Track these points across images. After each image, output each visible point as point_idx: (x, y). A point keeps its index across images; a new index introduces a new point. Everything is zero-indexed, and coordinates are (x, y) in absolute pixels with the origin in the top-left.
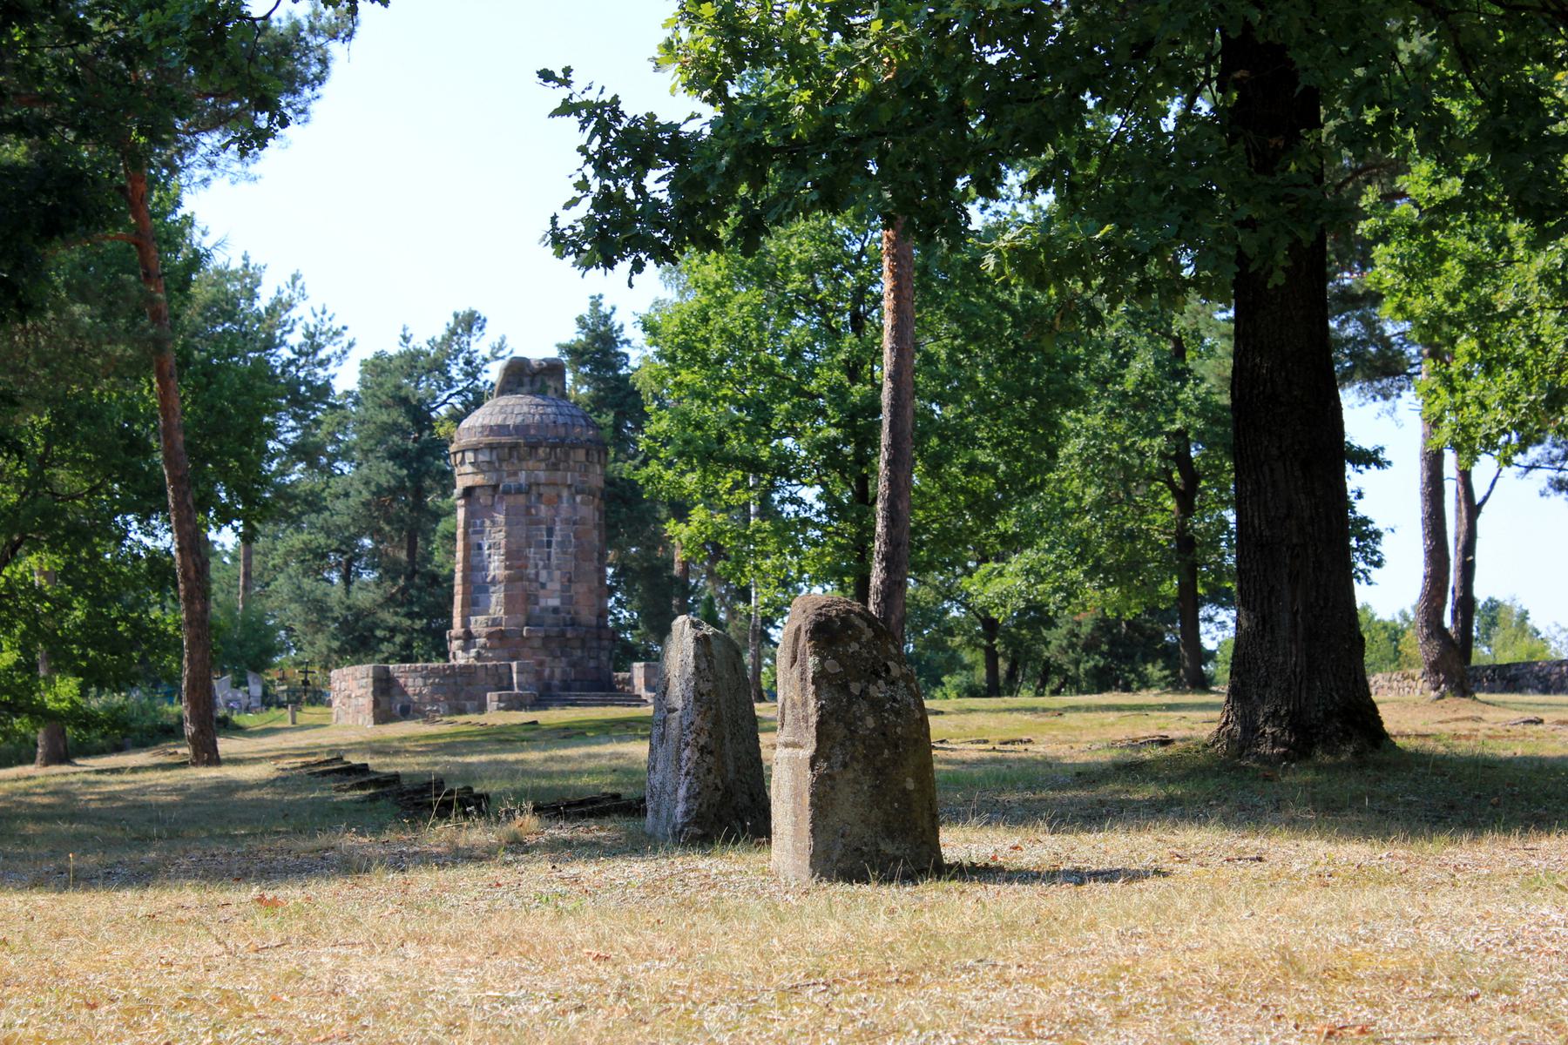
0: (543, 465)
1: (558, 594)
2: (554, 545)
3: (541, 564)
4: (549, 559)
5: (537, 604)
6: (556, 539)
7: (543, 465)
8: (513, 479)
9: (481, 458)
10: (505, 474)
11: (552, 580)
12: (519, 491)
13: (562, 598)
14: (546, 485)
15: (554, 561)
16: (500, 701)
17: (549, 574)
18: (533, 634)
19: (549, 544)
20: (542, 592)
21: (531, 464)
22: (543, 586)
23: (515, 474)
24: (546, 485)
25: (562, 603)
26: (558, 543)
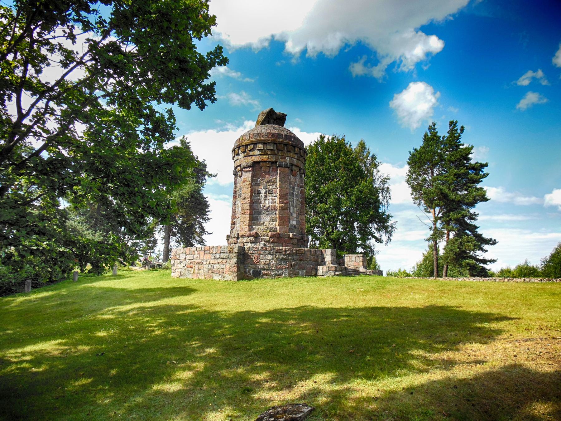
0: (296, 157)
1: (295, 219)
6: (295, 193)
8: (283, 160)
9: (268, 147)
10: (280, 157)
12: (286, 167)
13: (296, 221)
14: (296, 166)
16: (336, 271)
17: (293, 209)
19: (293, 196)
20: (291, 217)
23: (285, 158)
24: (296, 166)
26: (297, 195)
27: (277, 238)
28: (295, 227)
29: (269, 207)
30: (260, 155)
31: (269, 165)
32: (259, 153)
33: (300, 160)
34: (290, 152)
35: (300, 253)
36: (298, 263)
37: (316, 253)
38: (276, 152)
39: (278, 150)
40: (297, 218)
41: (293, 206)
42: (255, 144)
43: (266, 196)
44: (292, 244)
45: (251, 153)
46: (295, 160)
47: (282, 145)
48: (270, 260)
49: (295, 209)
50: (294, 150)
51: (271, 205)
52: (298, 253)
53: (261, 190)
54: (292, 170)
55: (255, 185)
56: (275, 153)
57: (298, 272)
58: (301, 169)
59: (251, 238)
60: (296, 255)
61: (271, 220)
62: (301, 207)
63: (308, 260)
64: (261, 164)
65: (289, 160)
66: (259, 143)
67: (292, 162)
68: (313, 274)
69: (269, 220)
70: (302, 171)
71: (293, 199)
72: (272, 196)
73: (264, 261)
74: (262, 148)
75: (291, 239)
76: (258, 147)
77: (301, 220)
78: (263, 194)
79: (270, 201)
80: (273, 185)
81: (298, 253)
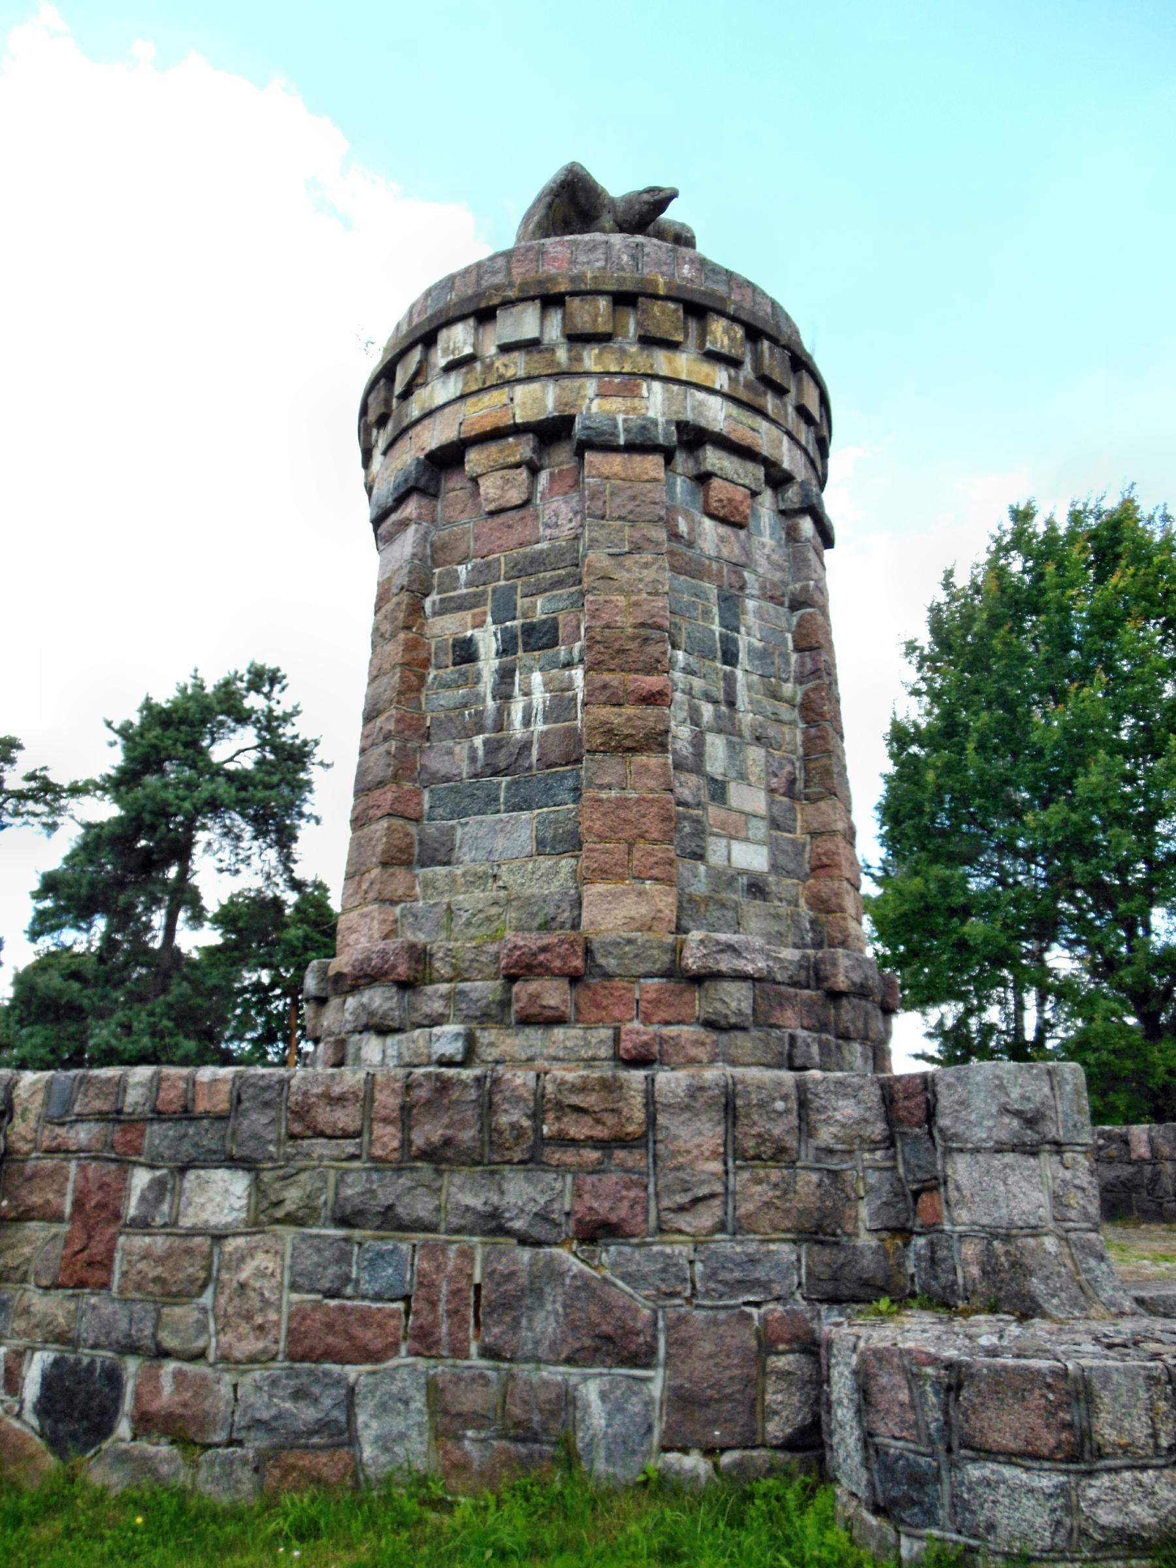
1: (759, 829)
2: (742, 656)
3: (707, 711)
4: (731, 704)
5: (700, 857)
7: (720, 377)
10: (591, 387)
11: (742, 777)
15: (746, 718)
18: (725, 964)
19: (730, 658)
20: (714, 813)
21: (684, 363)
22: (718, 789)
25: (775, 867)
26: (761, 656)
27: (564, 984)
28: (757, 888)
29: (526, 746)
30: (462, 397)
31: (523, 448)
32: (451, 387)
33: (761, 412)
34: (672, 346)
35: (578, 1129)
36: (554, 1273)
37: (806, 1129)
38: (562, 355)
39: (577, 339)
40: (775, 824)
41: (727, 727)
42: (428, 339)
43: (505, 675)
44: (710, 1024)
45: (415, 409)
46: (715, 402)
47: (603, 303)
48: (218, 1237)
49: (755, 754)
50: (703, 334)
51: (539, 727)
52: (565, 1141)
53: (478, 634)
54: (703, 479)
55: (445, 608)
56: (553, 363)
57: (567, 1400)
58: (778, 479)
59: (378, 998)
60: (533, 1161)
61: (541, 842)
62: (808, 741)
63: (706, 1218)
64: (474, 459)
65: (669, 399)
66: (449, 323)
67: (689, 416)
68: (775, 1429)
69: (531, 847)
70: (792, 494)
71: (730, 680)
72: (554, 664)
73: (160, 1244)
74: (468, 350)
75: (698, 980)
76: (446, 351)
77: (814, 834)
78: (488, 664)
79: (539, 697)
80: (558, 583)
81: (565, 1141)
